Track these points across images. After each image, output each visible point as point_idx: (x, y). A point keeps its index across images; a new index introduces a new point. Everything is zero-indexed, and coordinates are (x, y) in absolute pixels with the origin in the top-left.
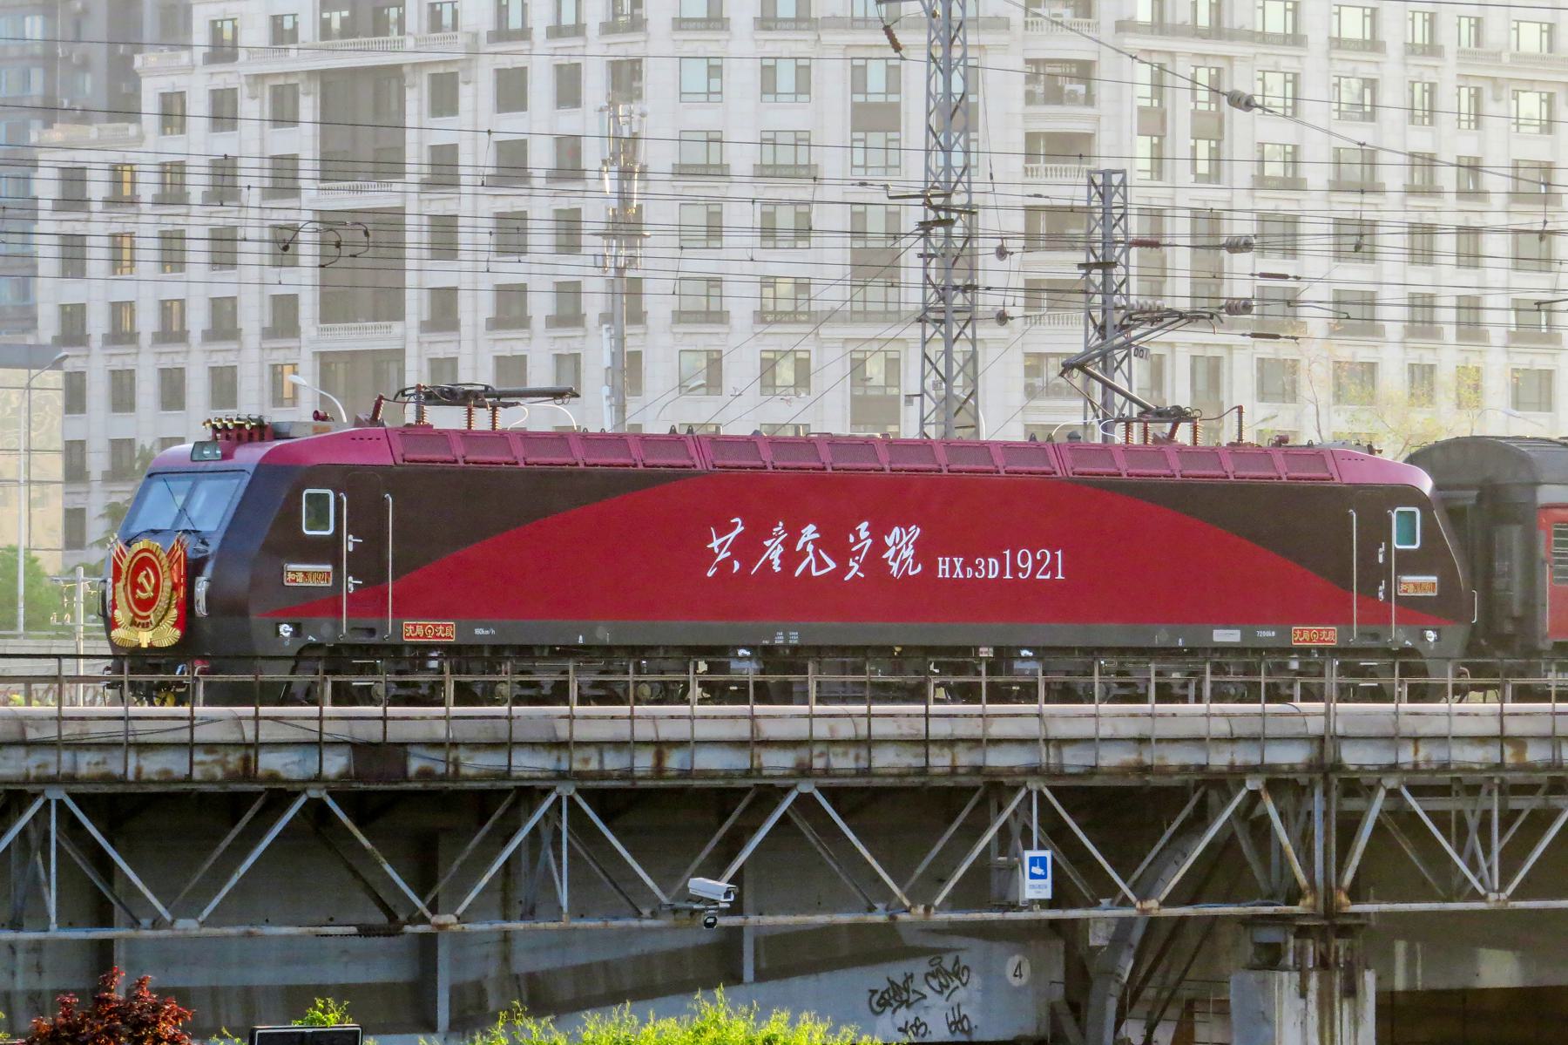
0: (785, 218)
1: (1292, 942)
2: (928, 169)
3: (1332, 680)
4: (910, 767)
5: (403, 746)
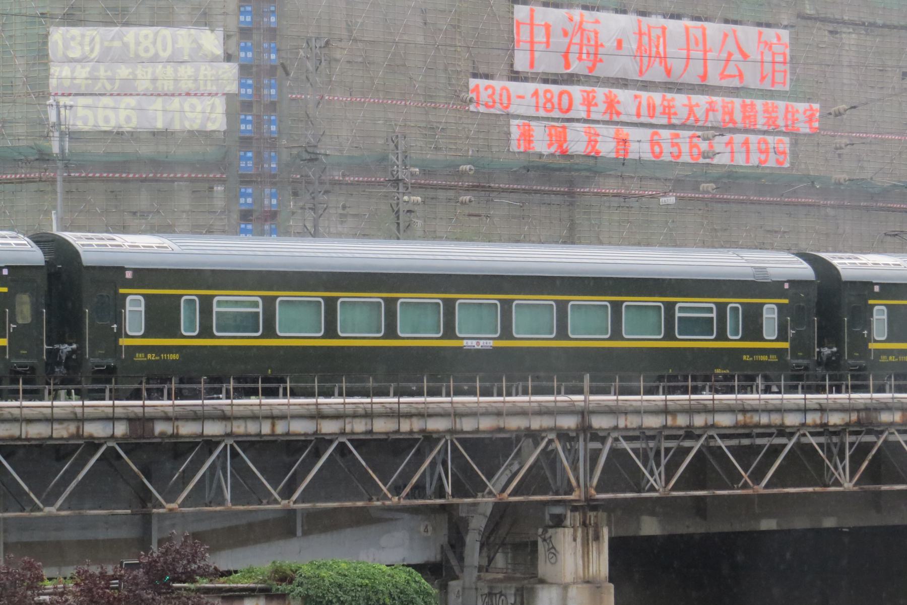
1: (569, 514)
5: (152, 419)
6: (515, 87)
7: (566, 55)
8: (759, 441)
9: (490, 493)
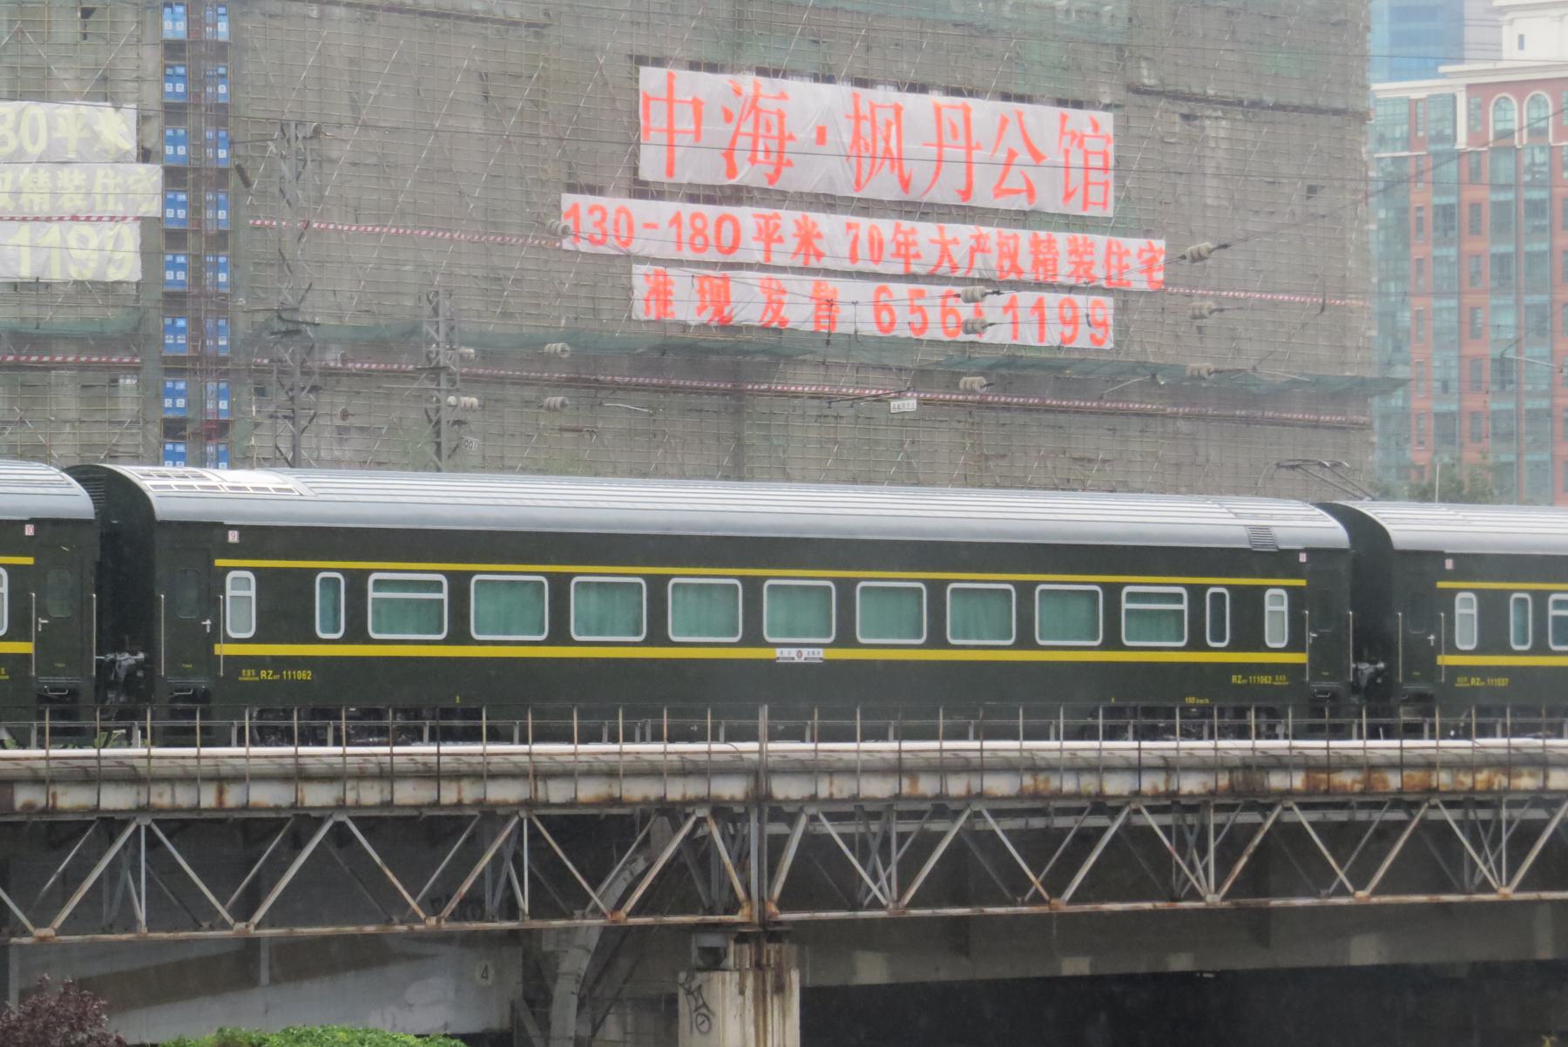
1: (732, 947)
3: (763, 721)
6: (642, 209)
7: (729, 154)
8: (1060, 822)
9: (596, 911)
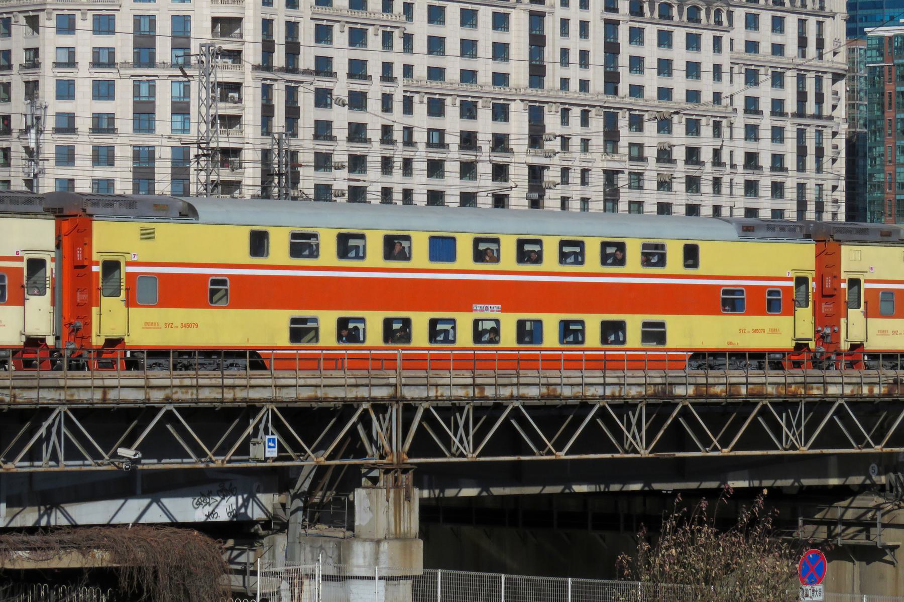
0: (103, 152)
2: (199, 131)
4: (215, 399)
